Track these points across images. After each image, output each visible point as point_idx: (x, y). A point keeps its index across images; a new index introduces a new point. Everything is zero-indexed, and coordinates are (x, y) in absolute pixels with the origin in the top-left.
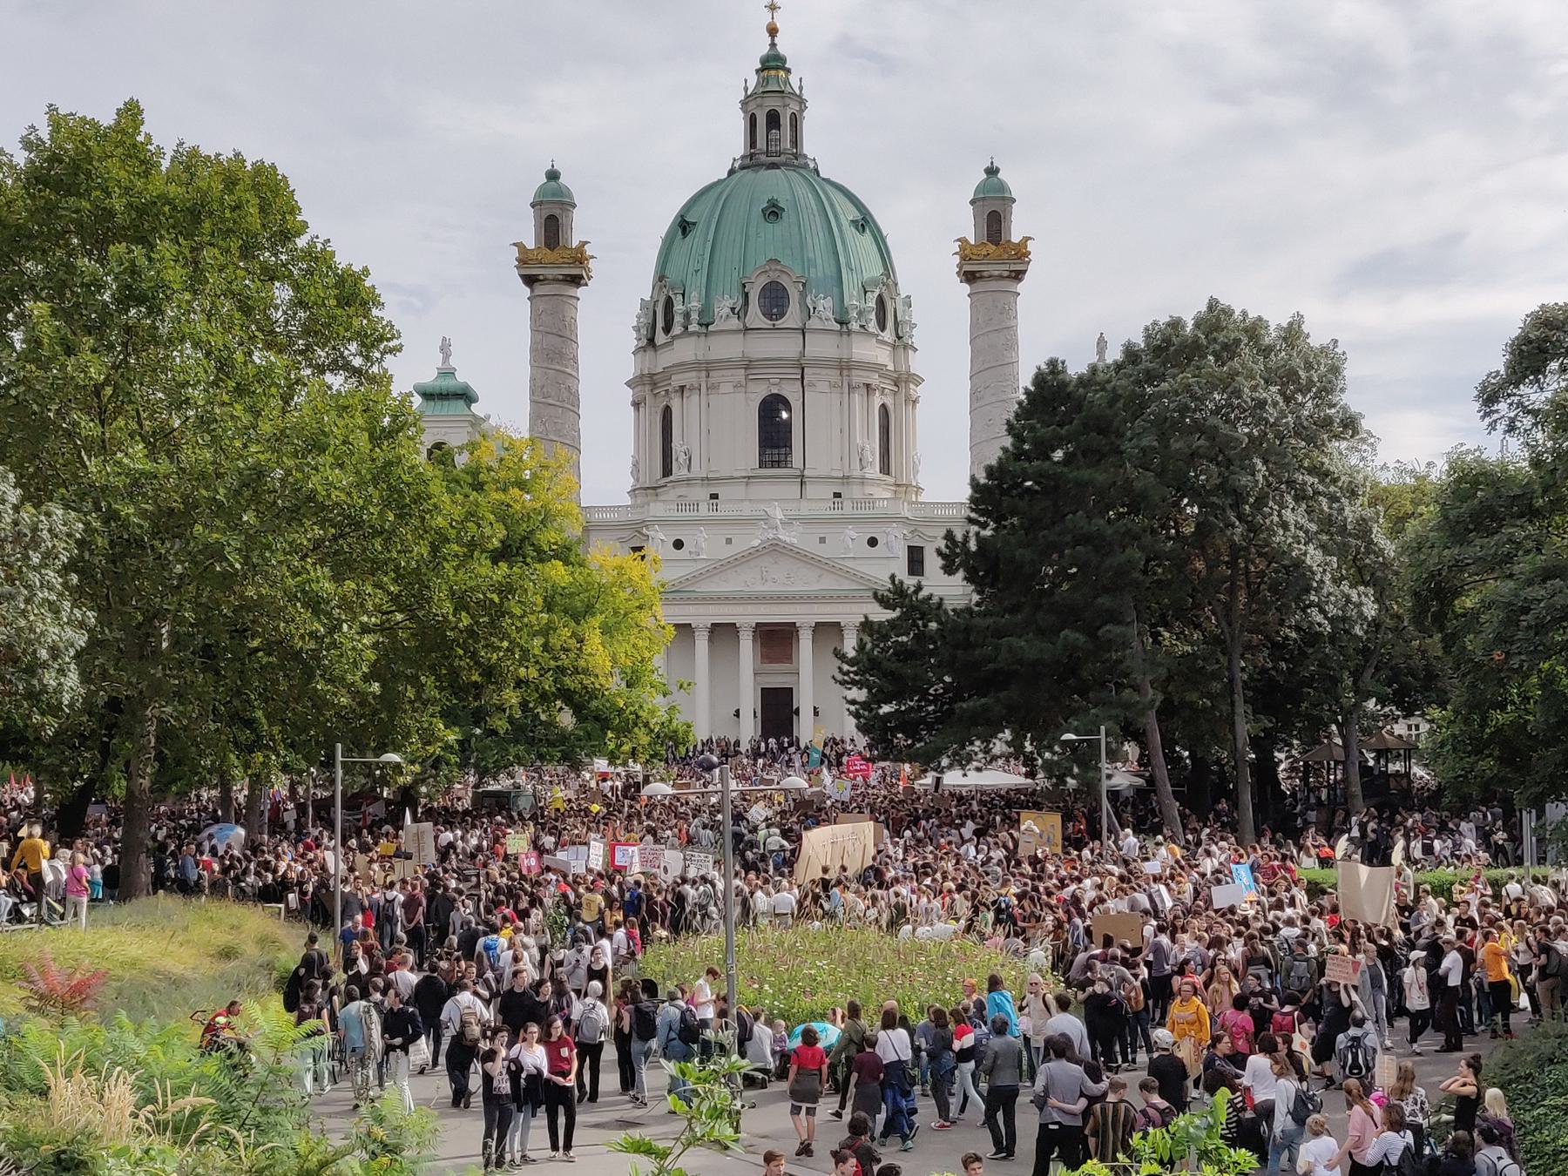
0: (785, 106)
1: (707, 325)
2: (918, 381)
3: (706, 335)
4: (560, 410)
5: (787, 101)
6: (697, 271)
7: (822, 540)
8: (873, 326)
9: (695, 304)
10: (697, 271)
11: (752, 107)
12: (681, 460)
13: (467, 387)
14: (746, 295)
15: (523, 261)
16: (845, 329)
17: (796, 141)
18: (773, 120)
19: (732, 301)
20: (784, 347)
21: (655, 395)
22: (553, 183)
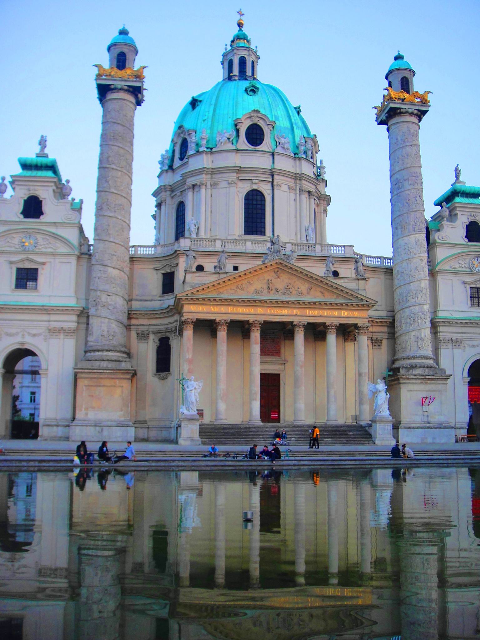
0: (249, 55)
1: (211, 149)
2: (328, 204)
3: (212, 153)
4: (120, 173)
5: (251, 52)
6: (204, 121)
10: (204, 121)
11: (229, 57)
13: (55, 162)
14: (238, 131)
15: (99, 76)
16: (297, 156)
17: (253, 74)
18: (243, 62)
20: (263, 162)
21: (172, 198)
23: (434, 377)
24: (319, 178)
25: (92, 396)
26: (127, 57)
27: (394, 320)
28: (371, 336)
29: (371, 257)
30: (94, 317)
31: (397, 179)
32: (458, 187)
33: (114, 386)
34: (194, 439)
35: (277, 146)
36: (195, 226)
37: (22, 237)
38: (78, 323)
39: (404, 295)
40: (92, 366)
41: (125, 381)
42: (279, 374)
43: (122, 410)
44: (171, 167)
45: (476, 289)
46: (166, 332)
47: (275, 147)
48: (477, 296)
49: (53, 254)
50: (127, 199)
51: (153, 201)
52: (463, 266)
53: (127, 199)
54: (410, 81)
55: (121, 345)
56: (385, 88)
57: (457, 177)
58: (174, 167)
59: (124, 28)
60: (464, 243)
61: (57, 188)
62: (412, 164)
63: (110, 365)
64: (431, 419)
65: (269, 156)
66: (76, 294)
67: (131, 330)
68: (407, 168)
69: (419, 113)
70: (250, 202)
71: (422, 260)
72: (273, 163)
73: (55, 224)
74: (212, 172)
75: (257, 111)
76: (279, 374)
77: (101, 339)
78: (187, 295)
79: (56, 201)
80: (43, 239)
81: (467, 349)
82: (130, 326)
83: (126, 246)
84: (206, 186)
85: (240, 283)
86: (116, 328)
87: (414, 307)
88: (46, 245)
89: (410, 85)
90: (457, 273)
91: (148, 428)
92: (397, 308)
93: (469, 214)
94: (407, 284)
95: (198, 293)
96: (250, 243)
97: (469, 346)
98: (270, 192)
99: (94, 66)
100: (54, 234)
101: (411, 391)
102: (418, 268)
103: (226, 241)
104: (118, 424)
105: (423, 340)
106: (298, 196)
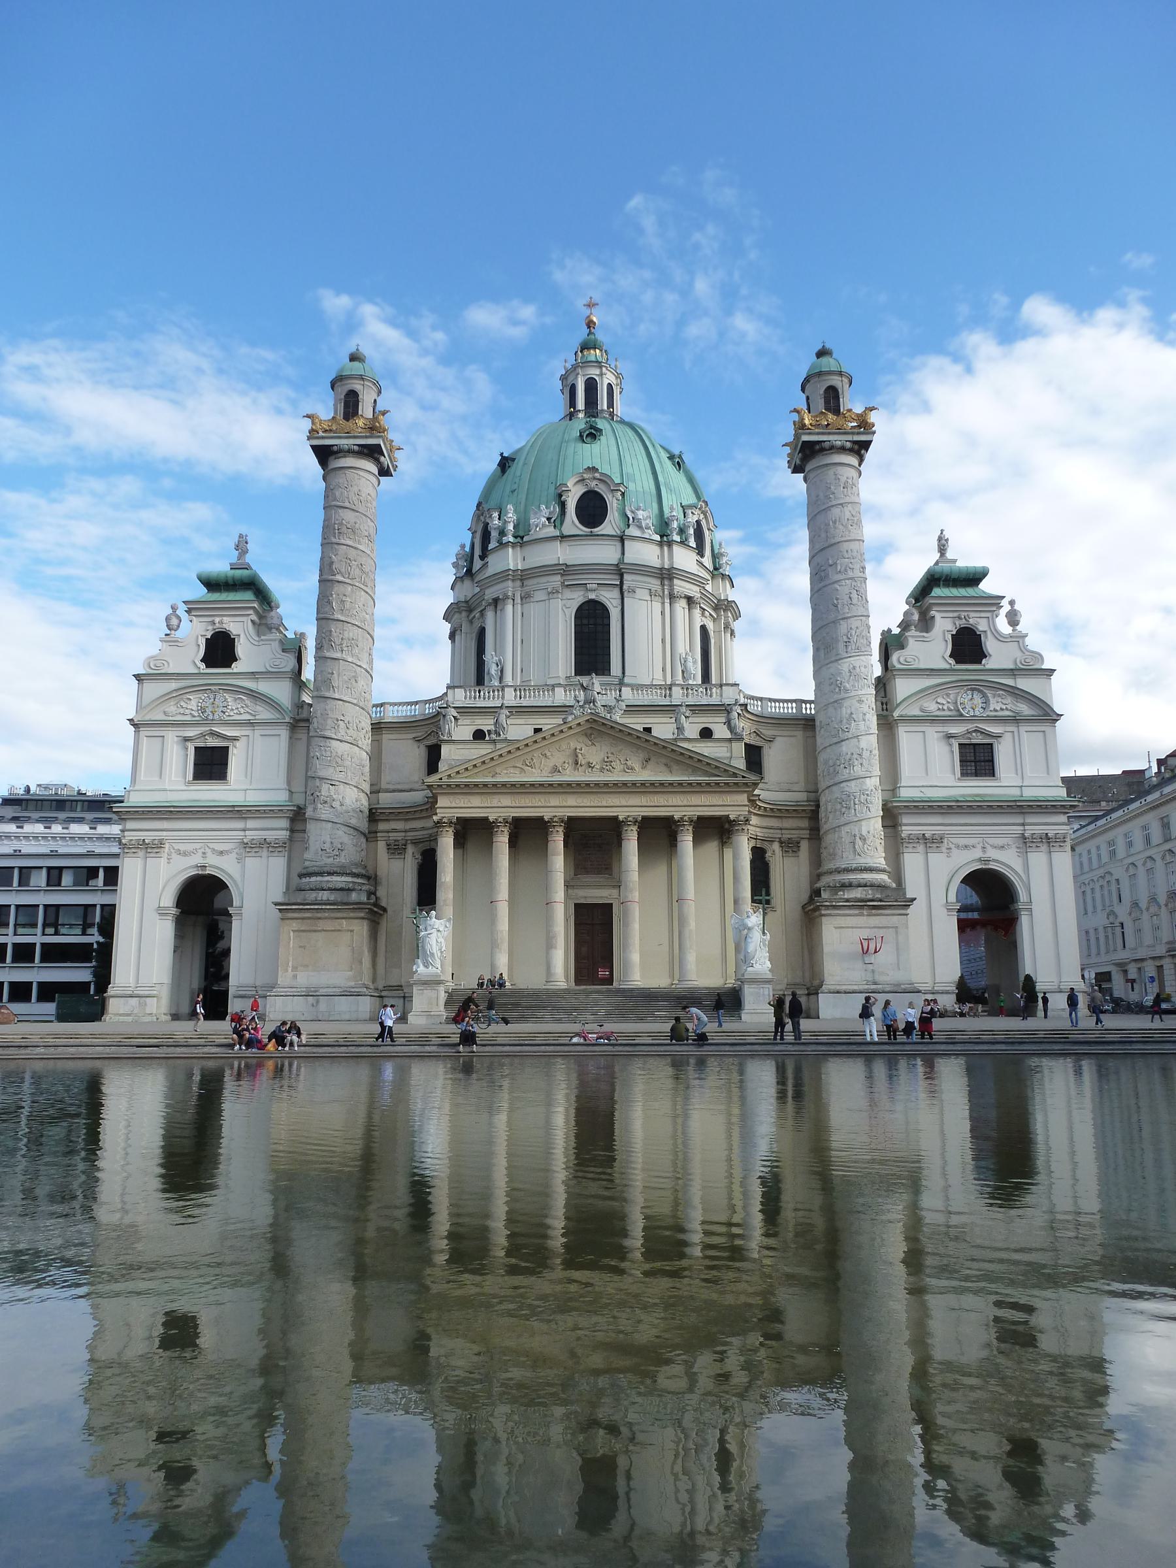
0: (601, 375)
1: (522, 538)
2: (737, 616)
3: (522, 545)
4: (349, 588)
6: (515, 490)
7: (648, 730)
8: (693, 543)
9: (511, 516)
10: (513, 492)
11: (570, 380)
12: (493, 672)
14: (563, 505)
15: (312, 434)
16: (665, 539)
17: (611, 404)
18: (591, 386)
19: (547, 511)
20: (606, 554)
21: (471, 622)
22: (356, 364)
23: (884, 903)
24: (716, 573)
25: (304, 947)
26: (361, 397)
27: (818, 806)
28: (780, 836)
29: (775, 701)
30: (311, 821)
31: (818, 564)
32: (945, 567)
33: (339, 930)
34: (432, 1013)
35: (629, 526)
36: (497, 664)
37: (203, 698)
38: (292, 831)
39: (831, 763)
40: (305, 900)
41: (356, 921)
42: (611, 905)
43: (351, 971)
44: (469, 573)
45: (972, 747)
46: (430, 841)
47: (622, 526)
48: (973, 758)
49: (250, 724)
50: (362, 628)
51: (447, 627)
52: (945, 708)
53: (362, 628)
54: (840, 393)
55: (356, 864)
56: (792, 409)
57: (942, 550)
58: (474, 571)
59: (357, 350)
60: (948, 667)
61: (261, 617)
62: (842, 536)
63: (332, 897)
64: (879, 978)
65: (616, 543)
66: (289, 783)
67: (379, 839)
68: (835, 544)
69: (856, 447)
70: (585, 621)
71: (861, 701)
72: (623, 554)
73: (253, 675)
74: (521, 576)
75: (594, 469)
76: (611, 905)
77: (321, 856)
78: (441, 779)
79: (257, 639)
80: (236, 699)
81: (955, 851)
82: (376, 832)
83: (361, 704)
84: (514, 600)
85: (529, 757)
86: (344, 837)
87: (848, 784)
88: (242, 711)
89: (841, 400)
90: (933, 720)
91: (404, 997)
92: (822, 785)
93: (956, 614)
94: (836, 743)
95: (459, 776)
96: (629, 689)
97: (958, 847)
98: (617, 602)
99: (304, 417)
100: (252, 691)
101: (843, 927)
102: (853, 716)
103: (546, 688)
104: (344, 991)
105: (865, 840)
106: (667, 605)
